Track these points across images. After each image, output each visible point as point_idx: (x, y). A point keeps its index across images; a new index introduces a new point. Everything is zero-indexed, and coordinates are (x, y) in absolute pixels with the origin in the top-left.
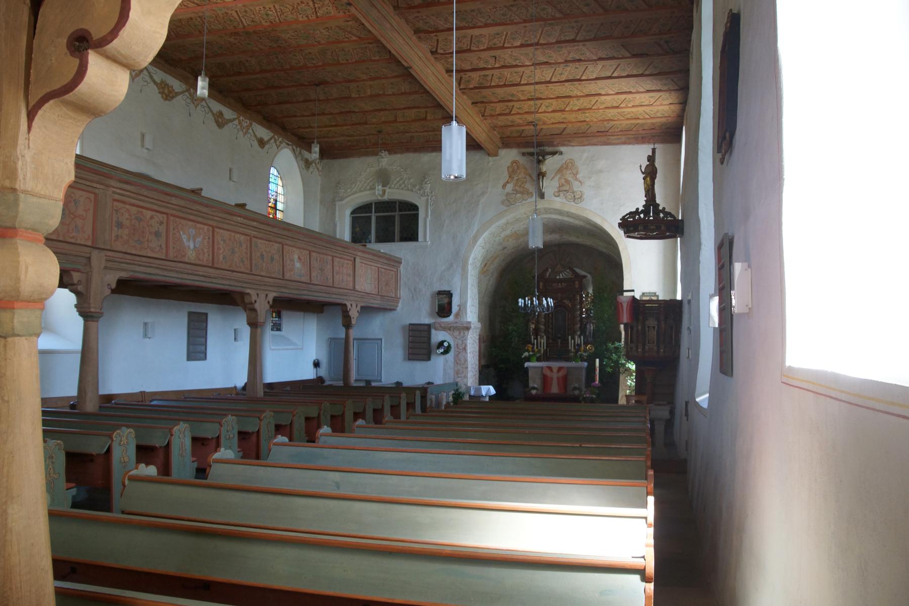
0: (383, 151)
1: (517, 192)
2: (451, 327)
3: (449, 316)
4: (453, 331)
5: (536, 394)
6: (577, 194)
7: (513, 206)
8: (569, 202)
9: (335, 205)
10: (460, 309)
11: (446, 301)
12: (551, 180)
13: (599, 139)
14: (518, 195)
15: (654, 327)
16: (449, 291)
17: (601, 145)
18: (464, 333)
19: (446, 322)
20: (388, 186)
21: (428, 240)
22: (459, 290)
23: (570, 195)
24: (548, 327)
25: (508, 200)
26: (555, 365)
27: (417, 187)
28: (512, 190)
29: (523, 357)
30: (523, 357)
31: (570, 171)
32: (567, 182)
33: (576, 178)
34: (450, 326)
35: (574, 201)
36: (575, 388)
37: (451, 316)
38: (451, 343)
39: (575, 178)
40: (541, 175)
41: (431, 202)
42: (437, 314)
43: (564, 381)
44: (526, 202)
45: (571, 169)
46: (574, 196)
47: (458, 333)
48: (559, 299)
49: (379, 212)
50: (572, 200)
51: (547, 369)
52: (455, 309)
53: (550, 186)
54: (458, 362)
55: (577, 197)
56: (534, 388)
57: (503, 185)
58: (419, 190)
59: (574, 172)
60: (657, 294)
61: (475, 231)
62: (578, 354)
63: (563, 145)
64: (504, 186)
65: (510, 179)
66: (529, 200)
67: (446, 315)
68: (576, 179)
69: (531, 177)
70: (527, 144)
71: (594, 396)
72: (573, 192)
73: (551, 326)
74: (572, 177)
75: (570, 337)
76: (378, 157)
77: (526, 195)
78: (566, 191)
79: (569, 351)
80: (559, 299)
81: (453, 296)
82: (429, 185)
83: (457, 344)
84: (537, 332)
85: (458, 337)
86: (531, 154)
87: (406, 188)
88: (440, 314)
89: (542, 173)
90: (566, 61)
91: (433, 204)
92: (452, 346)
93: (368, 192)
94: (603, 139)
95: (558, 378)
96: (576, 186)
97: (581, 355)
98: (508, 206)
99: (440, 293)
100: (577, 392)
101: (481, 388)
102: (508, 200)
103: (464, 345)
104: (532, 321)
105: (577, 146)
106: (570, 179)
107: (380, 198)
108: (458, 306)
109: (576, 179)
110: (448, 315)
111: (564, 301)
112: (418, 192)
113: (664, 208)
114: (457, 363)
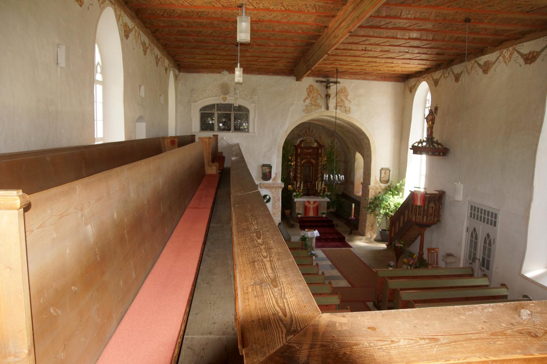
0: (225, 71)
1: (312, 105)
2: (271, 187)
3: (269, 180)
4: (272, 189)
5: (301, 217)
6: (347, 108)
7: (309, 113)
8: (342, 112)
9: (191, 105)
10: (276, 176)
11: (267, 170)
12: (333, 98)
13: (361, 76)
14: (313, 107)
15: (432, 208)
16: (270, 165)
17: (362, 80)
18: (278, 190)
19: (268, 183)
20: (228, 95)
21: (256, 132)
22: (276, 164)
23: (343, 109)
25: (307, 110)
26: (312, 200)
27: (249, 97)
28: (310, 103)
31: (344, 94)
32: (342, 100)
33: (347, 98)
34: (270, 186)
35: (345, 113)
36: (323, 213)
37: (271, 180)
38: (270, 196)
39: (346, 98)
40: (328, 96)
41: (258, 108)
42: (261, 179)
43: (317, 209)
44: (317, 111)
45: (344, 92)
46: (346, 110)
47: (275, 190)
48: (309, 159)
49: (220, 110)
50: (344, 112)
51: (307, 203)
52: (273, 175)
53: (332, 103)
54: (275, 208)
55: (347, 110)
56: (300, 214)
57: (304, 100)
58: (250, 99)
59: (346, 94)
60: (389, 169)
61: (286, 128)
62: (325, 194)
63: (340, 78)
64: (305, 100)
65: (308, 96)
66: (319, 110)
67: (267, 179)
68: (347, 99)
69: (321, 96)
70: (318, 76)
71: (402, 245)
72: (345, 107)
74: (344, 98)
76: (221, 74)
77: (318, 107)
78: (341, 106)
81: (272, 167)
82: (257, 96)
83: (274, 197)
84: (295, 178)
85: (275, 193)
86: (321, 82)
87: (241, 97)
88: (264, 179)
89: (328, 94)
90: (399, 52)
91: (259, 109)
92: (271, 198)
93: (215, 98)
94: (363, 76)
95: (313, 208)
96: (347, 103)
97: (327, 194)
98: (307, 113)
99: (264, 166)
100: (324, 216)
101: (314, 233)
102: (307, 110)
103: (278, 197)
104: (293, 172)
105: (348, 79)
106: (343, 99)
107: (223, 102)
108: (275, 173)
109: (347, 99)
110: (269, 179)
111: (311, 160)
112: (249, 100)
113: (437, 141)
114: (274, 208)
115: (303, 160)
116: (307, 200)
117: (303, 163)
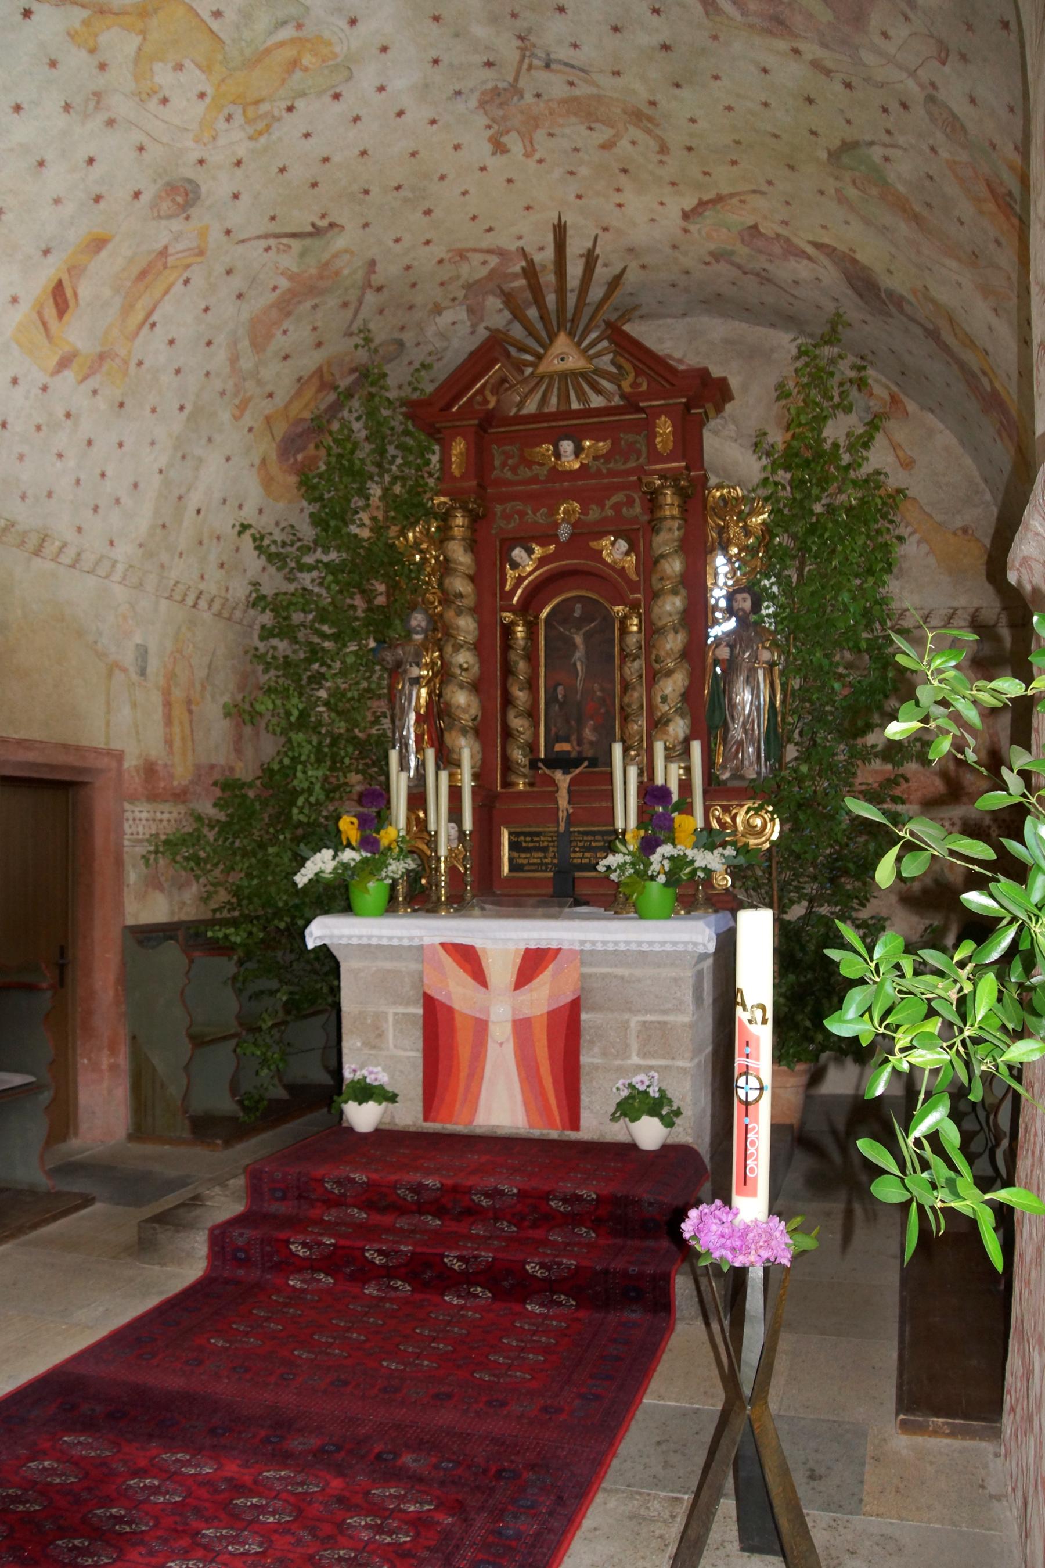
5: (383, 1136)
24: (508, 701)
29: (302, 879)
30: (302, 879)
48: (564, 532)
56: (366, 1092)
73: (521, 696)
75: (617, 749)
79: (612, 840)
80: (564, 532)
95: (522, 1027)
97: (678, 862)
104: (415, 672)
115: (518, 553)
116: (438, 940)
117: (520, 580)
